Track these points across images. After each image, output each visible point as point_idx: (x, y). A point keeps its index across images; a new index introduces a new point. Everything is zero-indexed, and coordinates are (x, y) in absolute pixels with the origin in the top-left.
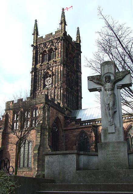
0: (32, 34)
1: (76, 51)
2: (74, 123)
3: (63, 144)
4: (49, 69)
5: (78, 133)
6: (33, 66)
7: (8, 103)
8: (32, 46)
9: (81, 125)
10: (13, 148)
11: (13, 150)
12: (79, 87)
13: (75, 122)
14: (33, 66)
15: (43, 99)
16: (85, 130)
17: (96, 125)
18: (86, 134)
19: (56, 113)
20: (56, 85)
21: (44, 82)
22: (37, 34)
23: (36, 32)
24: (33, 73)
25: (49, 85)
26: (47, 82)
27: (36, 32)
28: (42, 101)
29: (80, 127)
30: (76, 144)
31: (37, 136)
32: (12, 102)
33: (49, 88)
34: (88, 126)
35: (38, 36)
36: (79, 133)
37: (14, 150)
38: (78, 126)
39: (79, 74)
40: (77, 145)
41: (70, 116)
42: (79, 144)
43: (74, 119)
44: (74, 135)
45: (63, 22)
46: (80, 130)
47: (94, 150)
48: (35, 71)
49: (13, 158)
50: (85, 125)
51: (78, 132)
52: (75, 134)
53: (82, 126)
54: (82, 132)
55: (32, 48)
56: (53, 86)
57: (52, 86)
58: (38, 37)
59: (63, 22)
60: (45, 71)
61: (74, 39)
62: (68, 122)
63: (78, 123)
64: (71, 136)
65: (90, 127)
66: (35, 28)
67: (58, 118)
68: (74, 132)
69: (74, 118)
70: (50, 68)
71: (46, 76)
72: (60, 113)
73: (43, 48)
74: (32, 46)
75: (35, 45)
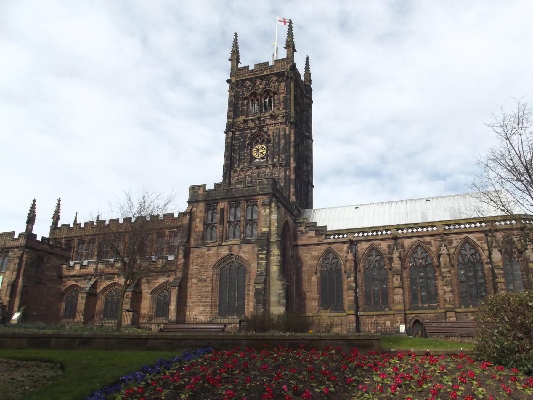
0: (230, 60)
1: (305, 99)
2: (312, 233)
3: (292, 272)
4: (261, 128)
5: (320, 252)
6: (231, 120)
7: (194, 190)
8: (229, 81)
9: (326, 238)
10: (207, 278)
11: (205, 281)
12: (310, 166)
13: (314, 232)
14: (231, 120)
15: (269, 186)
16: (334, 247)
17: (354, 239)
18: (336, 256)
19: (285, 214)
20: (275, 160)
21: (251, 151)
22: (237, 60)
23: (235, 57)
24: (230, 134)
25: (262, 158)
26: (258, 153)
27: (235, 57)
28: (266, 190)
29: (326, 241)
30: (316, 273)
31: (260, 256)
32: (202, 188)
33: (261, 163)
34: (340, 240)
35: (239, 64)
36: (323, 252)
37: (208, 280)
38: (322, 239)
39: (309, 141)
40: (319, 274)
41: (305, 221)
42: (322, 273)
43: (313, 226)
44: (314, 256)
45: (290, 46)
46: (325, 247)
47: (354, 285)
48: (230, 128)
49: (206, 297)
50: (334, 238)
51: (320, 250)
52: (315, 253)
53: (329, 241)
54: (328, 252)
55: (228, 85)
56: (270, 162)
57: (267, 161)
58: (240, 66)
59: (290, 46)
60: (254, 131)
61: (303, 78)
62: (302, 231)
63: (322, 235)
64: (306, 257)
65: (346, 242)
66: (235, 49)
67: (286, 223)
68: (313, 251)
69: (314, 224)
70: (263, 127)
71: (256, 139)
72: (288, 214)
73: (251, 88)
74: (229, 81)
75: (234, 80)
